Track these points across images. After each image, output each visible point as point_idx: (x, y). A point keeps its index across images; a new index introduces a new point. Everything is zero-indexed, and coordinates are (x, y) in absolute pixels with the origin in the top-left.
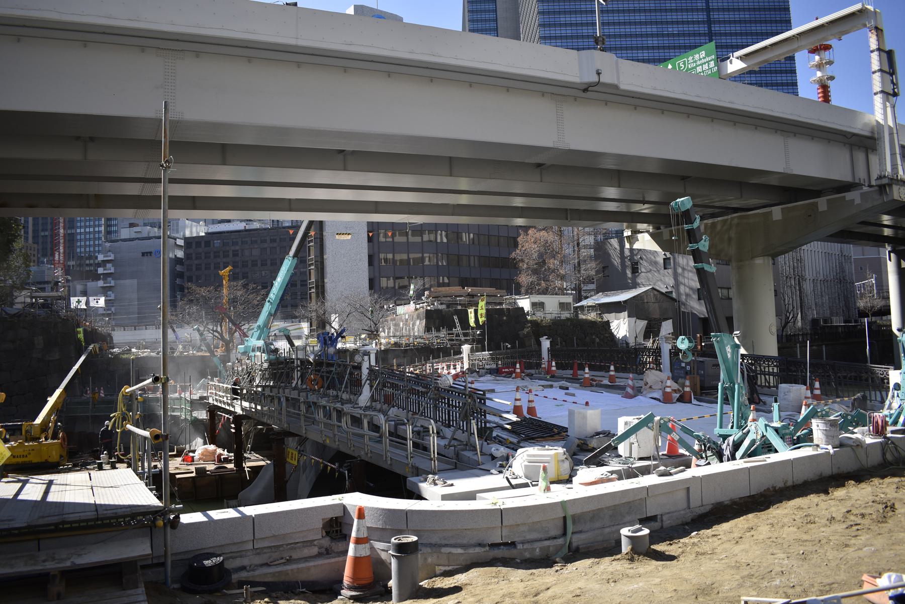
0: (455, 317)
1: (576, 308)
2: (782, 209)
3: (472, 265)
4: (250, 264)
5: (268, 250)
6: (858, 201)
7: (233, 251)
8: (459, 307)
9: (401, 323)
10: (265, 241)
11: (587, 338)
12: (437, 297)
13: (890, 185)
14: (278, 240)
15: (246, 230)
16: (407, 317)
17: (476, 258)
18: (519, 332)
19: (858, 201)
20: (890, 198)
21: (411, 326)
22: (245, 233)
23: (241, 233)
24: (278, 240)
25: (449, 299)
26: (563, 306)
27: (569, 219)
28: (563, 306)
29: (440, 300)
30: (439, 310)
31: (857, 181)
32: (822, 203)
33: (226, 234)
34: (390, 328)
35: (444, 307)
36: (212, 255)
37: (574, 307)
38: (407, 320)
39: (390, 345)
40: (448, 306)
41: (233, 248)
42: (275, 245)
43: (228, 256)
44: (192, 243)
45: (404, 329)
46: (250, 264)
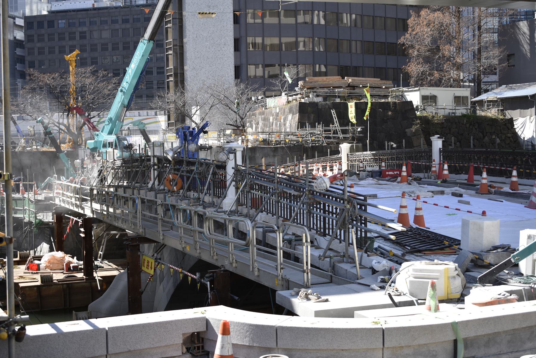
0: (333, 112)
1: (474, 103)
3: (354, 51)
4: (99, 48)
5: (120, 32)
7: (80, 33)
8: (338, 100)
9: (271, 118)
12: (312, 88)
14: (131, 21)
15: (94, 9)
16: (278, 111)
17: (358, 43)
18: (407, 130)
21: (282, 121)
22: (93, 12)
23: (89, 12)
24: (131, 21)
25: (326, 90)
26: (458, 100)
28: (458, 100)
29: (315, 92)
30: (314, 103)
34: (258, 123)
35: (319, 100)
36: (56, 37)
37: (471, 102)
38: (277, 114)
39: (258, 142)
40: (325, 98)
41: (80, 29)
42: (128, 26)
43: (74, 38)
44: (33, 23)
45: (274, 124)
46: (99, 48)
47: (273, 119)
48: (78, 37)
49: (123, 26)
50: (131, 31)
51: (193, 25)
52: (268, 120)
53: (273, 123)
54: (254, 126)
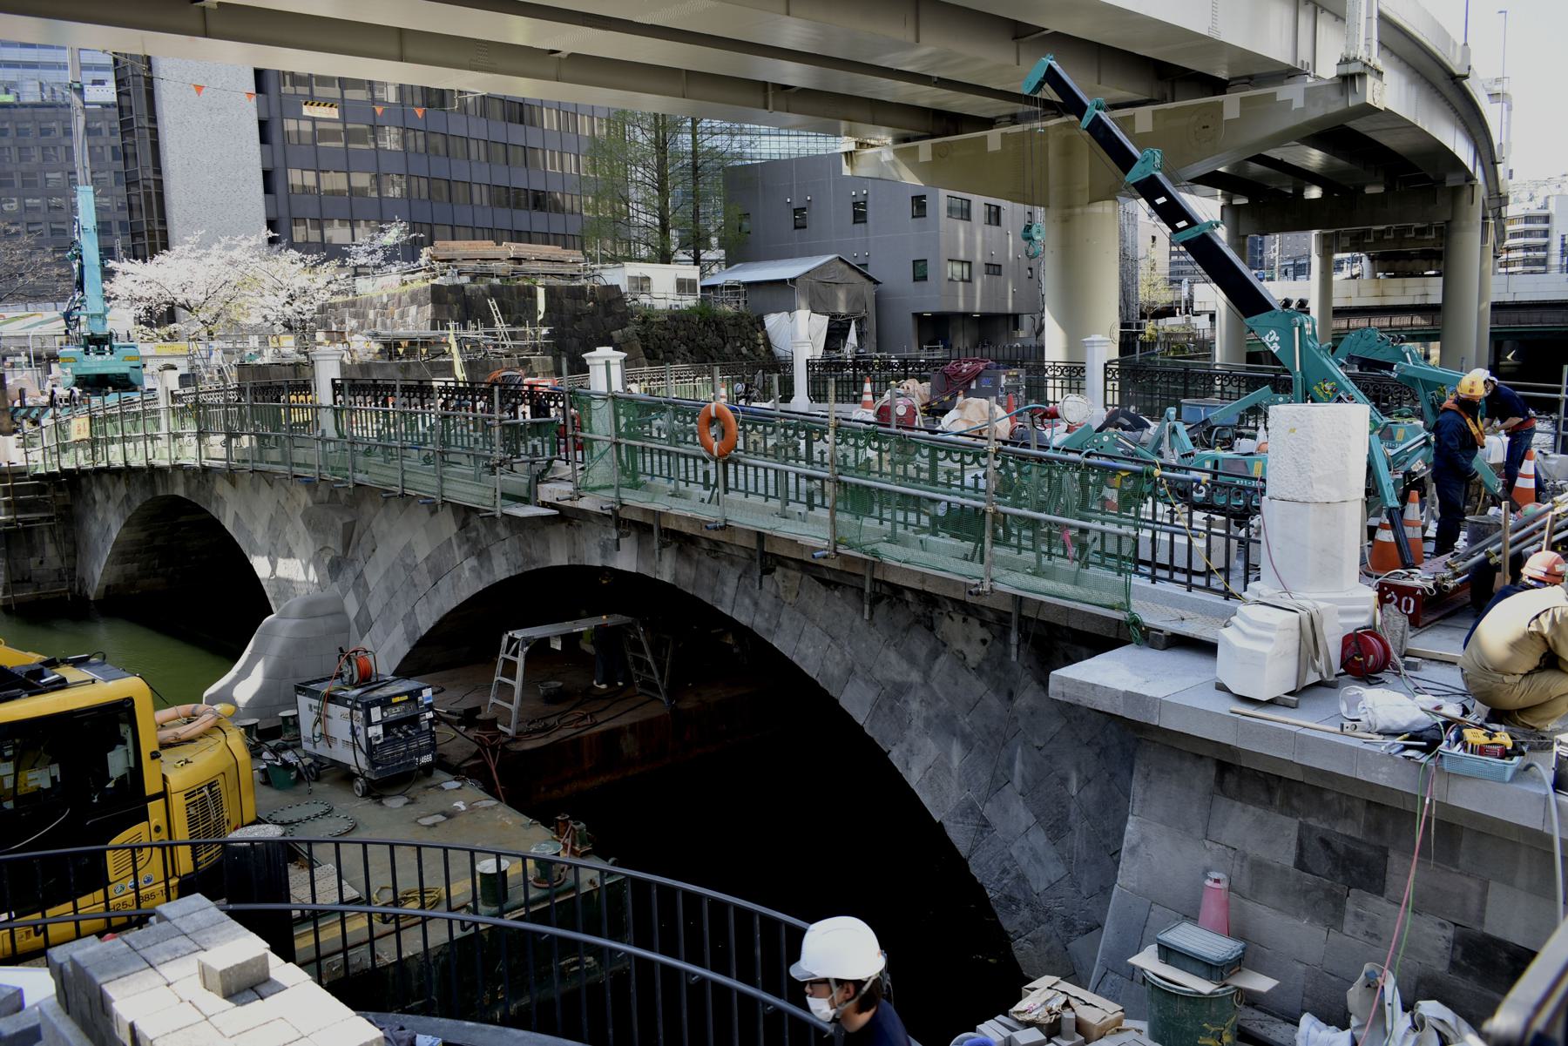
0: (492, 303)
2: (1154, 112)
3: (476, 200)
6: (1298, 103)
8: (496, 281)
9: (371, 314)
11: (728, 346)
12: (449, 261)
13: (1362, 75)
17: (484, 188)
18: (613, 333)
19: (1298, 103)
20: (1360, 101)
25: (473, 264)
27: (770, 106)
29: (455, 267)
30: (456, 286)
31: (1299, 67)
32: (1231, 104)
35: (465, 279)
38: (385, 306)
39: (371, 356)
40: (474, 278)
45: (378, 323)
52: (365, 316)
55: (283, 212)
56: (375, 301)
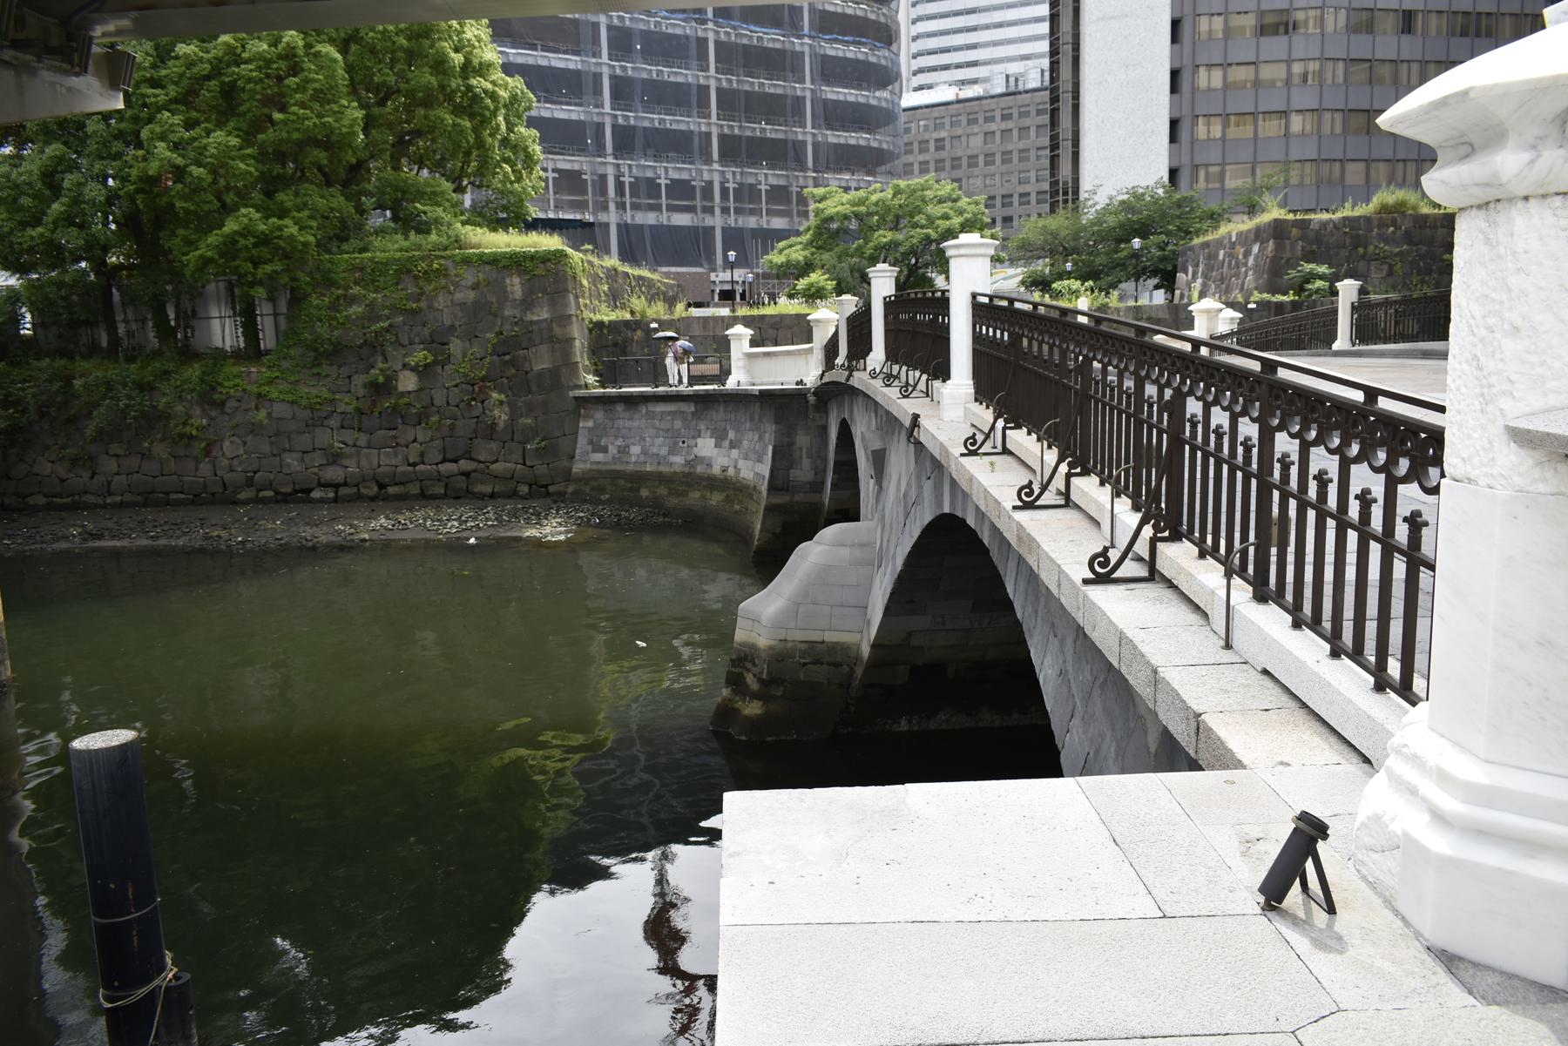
5: (998, 135)
10: (991, 119)
14: (1015, 115)
15: (959, 101)
16: (1234, 239)
21: (1241, 257)
24: (1015, 115)
33: (926, 110)
34: (1197, 265)
42: (1010, 124)
45: (1226, 263)
47: (1224, 255)
48: (932, 149)
49: (1003, 126)
50: (1015, 133)
51: (1097, 101)
53: (1224, 260)
54: (1190, 270)
55: (1185, 160)
56: (1226, 241)
